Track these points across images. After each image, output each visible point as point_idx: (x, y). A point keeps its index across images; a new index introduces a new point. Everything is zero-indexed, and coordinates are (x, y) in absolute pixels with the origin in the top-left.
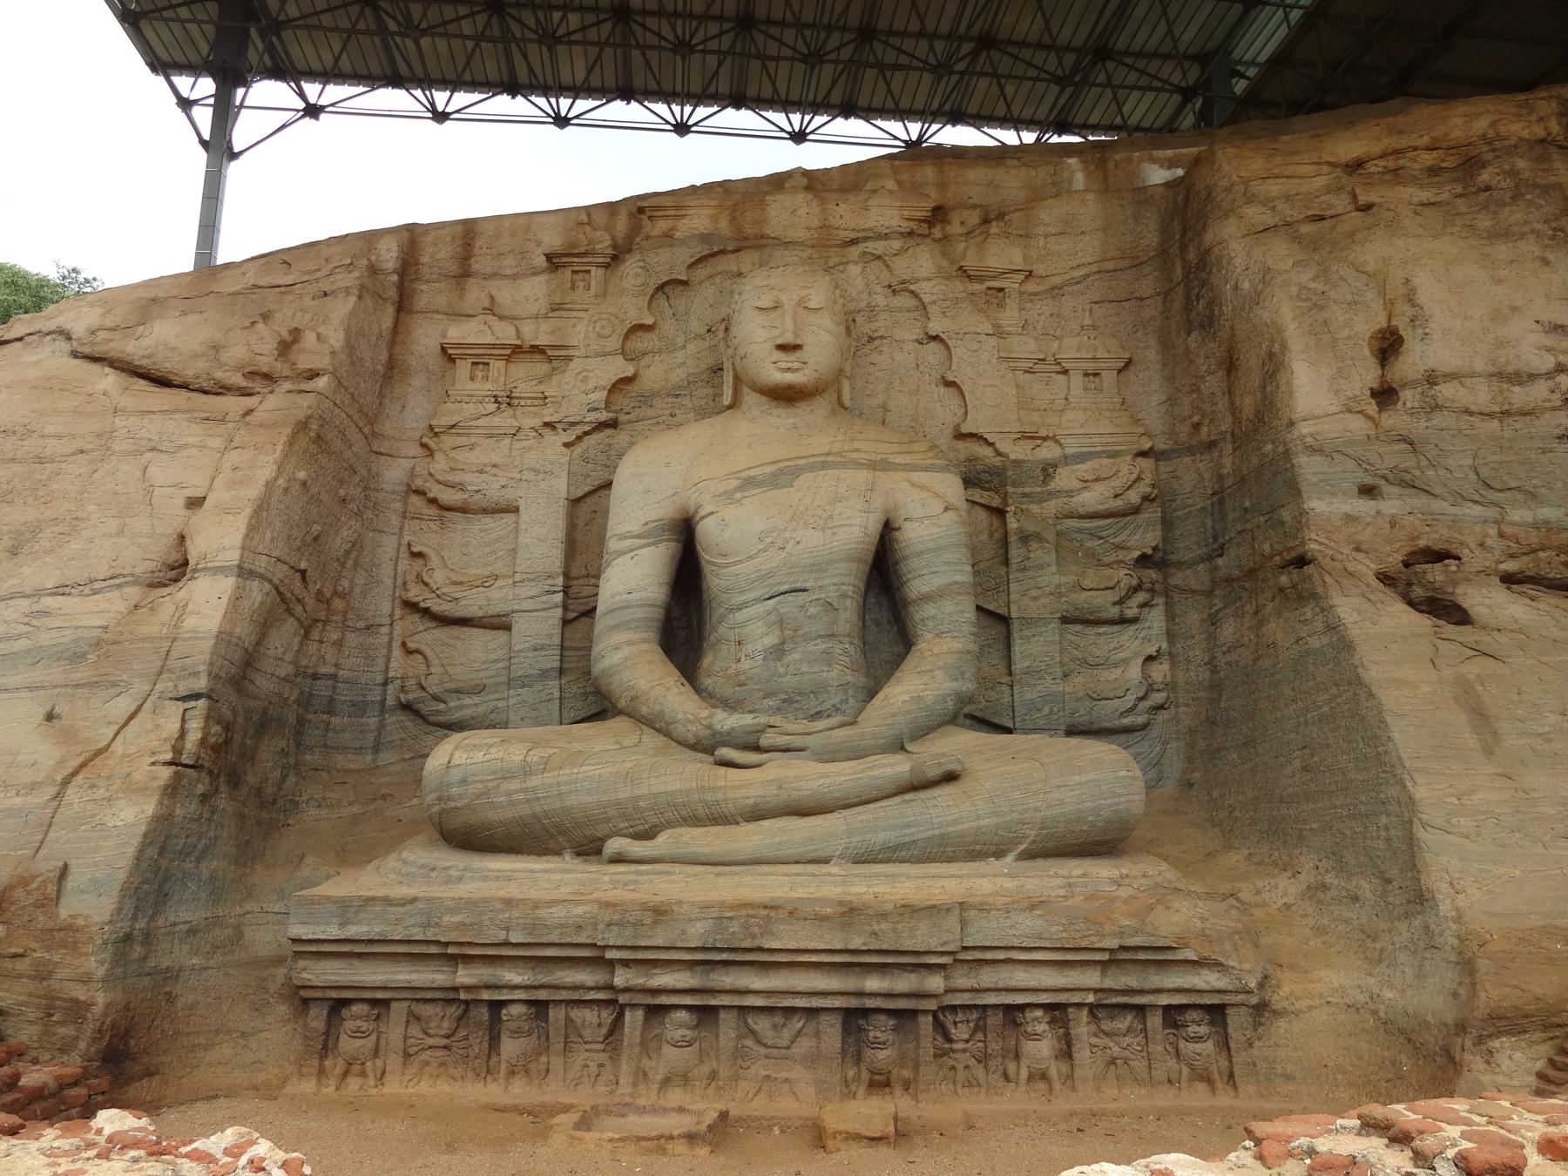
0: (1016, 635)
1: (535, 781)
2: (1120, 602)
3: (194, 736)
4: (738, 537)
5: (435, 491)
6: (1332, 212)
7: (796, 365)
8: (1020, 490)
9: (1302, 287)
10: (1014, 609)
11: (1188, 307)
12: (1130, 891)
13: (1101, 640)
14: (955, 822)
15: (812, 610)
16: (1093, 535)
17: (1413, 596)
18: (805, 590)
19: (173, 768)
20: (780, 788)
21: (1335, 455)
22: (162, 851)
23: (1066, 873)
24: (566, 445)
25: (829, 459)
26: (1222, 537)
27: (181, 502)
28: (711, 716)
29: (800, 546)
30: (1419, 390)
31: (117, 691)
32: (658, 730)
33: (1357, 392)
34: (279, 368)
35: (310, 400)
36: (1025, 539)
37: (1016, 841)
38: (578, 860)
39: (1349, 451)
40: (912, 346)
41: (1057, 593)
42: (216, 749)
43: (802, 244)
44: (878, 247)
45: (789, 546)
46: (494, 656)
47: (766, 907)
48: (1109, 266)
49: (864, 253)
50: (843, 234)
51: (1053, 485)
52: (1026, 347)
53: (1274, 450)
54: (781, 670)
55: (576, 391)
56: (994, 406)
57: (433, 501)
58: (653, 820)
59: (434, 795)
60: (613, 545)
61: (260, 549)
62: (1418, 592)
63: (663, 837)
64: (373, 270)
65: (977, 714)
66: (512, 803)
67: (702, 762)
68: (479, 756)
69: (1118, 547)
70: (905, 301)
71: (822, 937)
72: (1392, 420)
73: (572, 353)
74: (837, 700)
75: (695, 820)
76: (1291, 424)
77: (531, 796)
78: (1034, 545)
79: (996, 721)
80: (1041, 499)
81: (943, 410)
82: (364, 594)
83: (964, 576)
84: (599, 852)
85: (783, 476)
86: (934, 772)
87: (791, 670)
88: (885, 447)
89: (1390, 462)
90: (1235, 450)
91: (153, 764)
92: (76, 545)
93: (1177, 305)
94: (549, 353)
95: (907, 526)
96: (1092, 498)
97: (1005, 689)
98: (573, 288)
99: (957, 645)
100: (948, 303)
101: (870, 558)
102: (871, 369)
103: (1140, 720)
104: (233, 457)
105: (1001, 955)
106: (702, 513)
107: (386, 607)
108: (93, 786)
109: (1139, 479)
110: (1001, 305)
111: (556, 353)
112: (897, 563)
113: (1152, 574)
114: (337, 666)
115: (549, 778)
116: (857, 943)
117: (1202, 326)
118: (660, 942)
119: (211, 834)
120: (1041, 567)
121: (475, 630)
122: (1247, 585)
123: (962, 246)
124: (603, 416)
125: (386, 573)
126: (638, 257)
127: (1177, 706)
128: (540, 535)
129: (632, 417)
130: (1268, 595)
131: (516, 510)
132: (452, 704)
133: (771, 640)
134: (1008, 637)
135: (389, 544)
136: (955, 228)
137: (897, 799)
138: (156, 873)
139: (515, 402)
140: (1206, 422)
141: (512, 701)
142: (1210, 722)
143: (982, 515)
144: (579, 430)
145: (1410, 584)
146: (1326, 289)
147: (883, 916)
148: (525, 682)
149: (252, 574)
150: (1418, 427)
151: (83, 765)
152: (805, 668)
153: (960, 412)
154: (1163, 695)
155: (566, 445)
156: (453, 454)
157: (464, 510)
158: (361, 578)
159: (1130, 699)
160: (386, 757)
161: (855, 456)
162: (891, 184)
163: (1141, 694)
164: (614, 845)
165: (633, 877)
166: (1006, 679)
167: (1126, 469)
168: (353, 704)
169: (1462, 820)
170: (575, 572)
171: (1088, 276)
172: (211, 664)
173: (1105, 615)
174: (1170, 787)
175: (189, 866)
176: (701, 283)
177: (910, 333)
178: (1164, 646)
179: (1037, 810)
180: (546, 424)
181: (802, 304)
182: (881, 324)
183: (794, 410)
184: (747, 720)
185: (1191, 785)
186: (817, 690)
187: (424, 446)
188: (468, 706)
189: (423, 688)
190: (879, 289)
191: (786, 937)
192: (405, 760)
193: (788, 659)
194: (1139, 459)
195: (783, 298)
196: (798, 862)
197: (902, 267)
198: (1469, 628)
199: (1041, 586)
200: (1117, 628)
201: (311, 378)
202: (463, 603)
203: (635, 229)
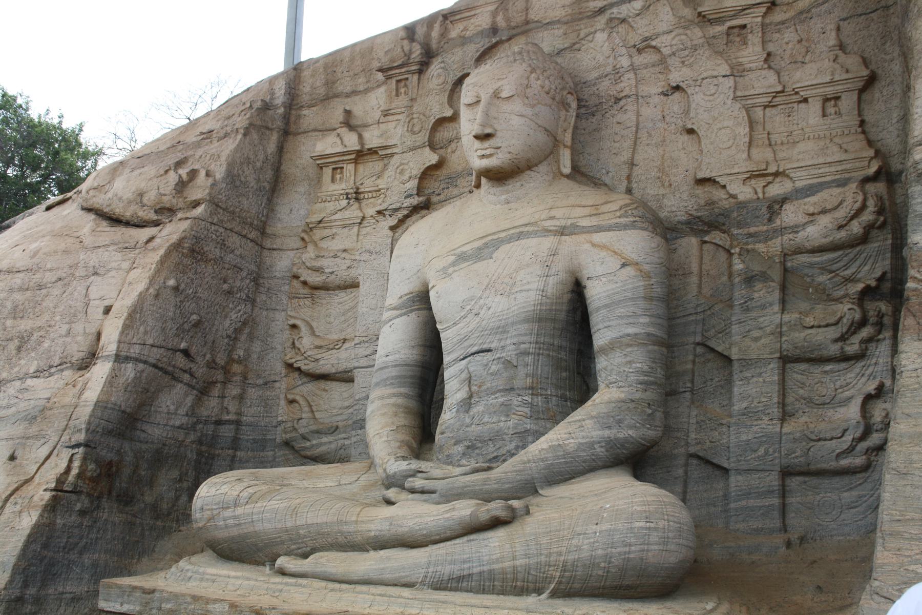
0: (735, 377)
1: (239, 511)
2: (843, 338)
3: (75, 471)
7: (488, 152)
8: (746, 231)
13: (826, 379)
14: (498, 561)
15: (494, 368)
16: (824, 269)
18: (489, 351)
19: (54, 493)
20: (391, 524)
22: (45, 546)
25: (526, 229)
27: (101, 310)
29: (490, 312)
31: (42, 441)
36: (749, 280)
40: (656, 99)
42: (95, 480)
43: (559, 22)
45: (482, 312)
46: (346, 404)
49: (611, 20)
51: (778, 222)
52: (763, 82)
54: (468, 420)
55: (396, 183)
57: (305, 283)
61: (135, 340)
65: (701, 454)
66: (226, 527)
70: (649, 57)
73: (395, 150)
78: (759, 286)
79: (715, 461)
80: (766, 238)
82: (261, 358)
85: (485, 249)
87: (476, 421)
88: (579, 212)
92: (46, 345)
94: (381, 153)
100: (687, 52)
102: (617, 128)
109: (864, 207)
111: (384, 152)
113: (884, 307)
114: (239, 414)
115: (248, 509)
119: (93, 536)
120: (763, 307)
121: (334, 383)
124: (415, 201)
126: (440, 59)
129: (442, 197)
132: (314, 442)
133: (462, 395)
137: (465, 538)
138: (41, 561)
139: (362, 196)
141: (354, 439)
144: (400, 215)
149: (127, 359)
151: (17, 489)
152: (485, 420)
156: (323, 244)
157: (325, 288)
158: (257, 347)
159: (848, 438)
161: (548, 224)
163: (858, 435)
164: (281, 561)
165: (280, 587)
167: (851, 196)
168: (255, 441)
172: (89, 423)
173: (825, 353)
175: (73, 556)
177: (654, 88)
179: (560, 554)
180: (379, 212)
181: (496, 95)
182: (627, 83)
183: (506, 188)
186: (496, 437)
187: (303, 239)
188: (325, 444)
190: (624, 51)
193: (474, 410)
196: (396, 585)
200: (843, 365)
201: (194, 207)
202: (321, 362)
203: (443, 35)
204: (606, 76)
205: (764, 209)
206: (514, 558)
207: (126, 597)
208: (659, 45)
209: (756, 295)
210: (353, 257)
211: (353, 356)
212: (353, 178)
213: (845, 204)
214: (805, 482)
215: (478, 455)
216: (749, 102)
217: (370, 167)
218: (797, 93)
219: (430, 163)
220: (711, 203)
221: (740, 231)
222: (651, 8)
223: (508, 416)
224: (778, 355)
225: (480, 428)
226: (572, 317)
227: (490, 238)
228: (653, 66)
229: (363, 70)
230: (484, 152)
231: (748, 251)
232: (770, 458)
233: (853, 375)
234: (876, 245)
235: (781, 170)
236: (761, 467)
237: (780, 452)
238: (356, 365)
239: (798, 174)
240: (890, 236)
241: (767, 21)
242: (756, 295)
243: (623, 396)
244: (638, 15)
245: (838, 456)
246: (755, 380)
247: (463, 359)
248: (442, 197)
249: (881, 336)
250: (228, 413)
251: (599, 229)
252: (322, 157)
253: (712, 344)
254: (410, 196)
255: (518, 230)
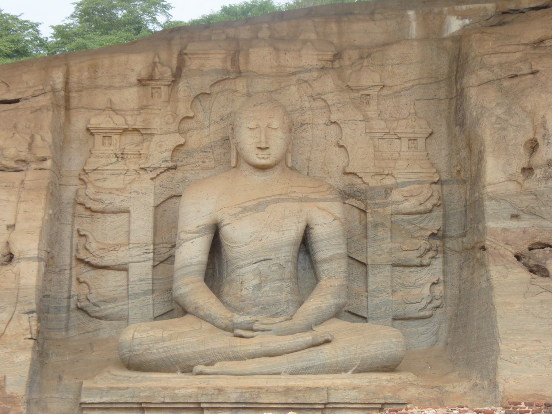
0: (370, 273)
1: (166, 344)
2: (421, 256)
3: (34, 328)
4: (241, 235)
5: (89, 204)
6: (521, 73)
7: (266, 156)
8: (374, 202)
9: (498, 117)
10: (369, 260)
11: (456, 113)
12: (393, 384)
14: (329, 359)
15: (274, 268)
16: (410, 223)
17: (530, 263)
21: (502, 201)
23: (369, 377)
24: (152, 179)
25: (281, 197)
26: (456, 232)
27: (5, 227)
28: (232, 317)
30: (544, 169)
32: (207, 321)
33: (515, 171)
34: (29, 157)
35: (47, 174)
36: (376, 226)
37: (352, 366)
38: (183, 375)
39: (508, 199)
40: (322, 127)
41: (390, 253)
43: (268, 75)
44: (306, 76)
46: (119, 284)
47: (258, 388)
48: (424, 81)
49: (299, 80)
50: (288, 69)
51: (390, 199)
52: (379, 126)
53: (479, 195)
54: (260, 295)
56: (362, 159)
57: (89, 209)
58: (213, 359)
59: (128, 350)
60: (183, 236)
62: (532, 262)
63: (218, 365)
64: (54, 91)
65: (351, 311)
66: (159, 353)
67: (228, 336)
68: (144, 335)
69: (422, 229)
71: (278, 398)
72: (530, 184)
73: (154, 132)
74: (284, 308)
75: (230, 359)
76: (484, 186)
77: (166, 350)
79: (359, 314)
80: (384, 206)
81: (338, 160)
83: (341, 250)
84: (191, 371)
85: (260, 206)
86: (321, 340)
89: (524, 204)
90: (471, 189)
91: (25, 339)
93: (453, 108)
94: (142, 132)
95: (316, 227)
96: (408, 205)
97: (364, 298)
98: (152, 96)
99: (337, 283)
100: (340, 105)
101: (299, 242)
103: (428, 313)
104: (23, 206)
105: (342, 406)
106: (225, 223)
107: (68, 261)
108: (6, 347)
109: (432, 196)
110: (368, 103)
111: (145, 132)
112: (312, 243)
113: (438, 242)
116: (290, 401)
117: (460, 125)
118: (220, 401)
120: (383, 240)
122: (472, 253)
123: (349, 72)
124: (170, 164)
125: (67, 245)
126: (185, 81)
127: (446, 307)
128: (142, 226)
129: (183, 163)
130: (476, 260)
131: (129, 212)
132: (102, 308)
133: (255, 282)
134: (367, 273)
135: (67, 230)
136: (346, 62)
137: (307, 350)
139: (125, 156)
140: (463, 170)
142: (456, 315)
143: (356, 212)
144: (158, 171)
145: (530, 258)
146: (508, 118)
147: (300, 391)
148: (136, 296)
150: (542, 187)
152: (271, 294)
153: (346, 161)
154: (440, 301)
155: (152, 179)
156: (98, 184)
157: (103, 212)
159: (424, 303)
160: (73, 333)
161: (293, 195)
162: (313, 36)
163: (429, 301)
166: (365, 294)
167: (426, 191)
168: (56, 308)
169: (516, 357)
170: (156, 243)
171: (413, 86)
174: (441, 345)
176: (217, 93)
177: (322, 120)
178: (441, 278)
179: (360, 354)
180: (142, 169)
181: (268, 126)
184: (247, 318)
185: (448, 344)
186: (276, 303)
187: (81, 179)
188: (110, 308)
189: (88, 300)
190: (306, 98)
191: (264, 399)
192: (80, 334)
193: (263, 290)
194: (434, 186)
195: (260, 124)
197: (318, 87)
198: (547, 279)
199: (381, 249)
200: (419, 269)
202: (106, 259)
204: (296, 111)
205: (383, 192)
206: (337, 357)
207: (104, 394)
208: (326, 99)
209: (379, 234)
210: (125, 195)
211: (128, 255)
212: (118, 144)
213: (423, 193)
214: (401, 323)
215: (267, 312)
216: (372, 135)
217: (128, 139)
218: (396, 134)
219: (180, 143)
220: (351, 185)
221: (371, 202)
222: (322, 78)
223: (281, 292)
224: (391, 263)
225: (267, 299)
226: (305, 244)
227: (261, 200)
228: (321, 108)
229: (119, 74)
230: (263, 156)
231: (375, 212)
232: (388, 312)
233: (424, 273)
234: (436, 213)
235: (390, 173)
236: (384, 317)
237: (392, 309)
238: (131, 260)
239: (399, 176)
240: (442, 210)
241: (379, 94)
242: (379, 234)
243: (339, 283)
244: (315, 80)
245: (419, 310)
246: (379, 275)
247: (255, 263)
248: (183, 163)
249: (437, 256)
250: (46, 290)
251: (320, 200)
252: (97, 128)
253: (353, 256)
254: (166, 161)
255: (276, 197)
